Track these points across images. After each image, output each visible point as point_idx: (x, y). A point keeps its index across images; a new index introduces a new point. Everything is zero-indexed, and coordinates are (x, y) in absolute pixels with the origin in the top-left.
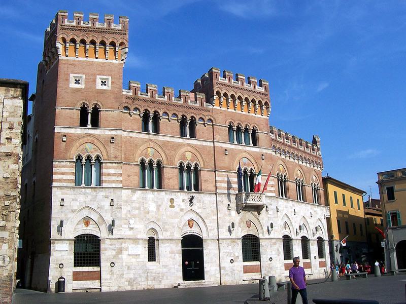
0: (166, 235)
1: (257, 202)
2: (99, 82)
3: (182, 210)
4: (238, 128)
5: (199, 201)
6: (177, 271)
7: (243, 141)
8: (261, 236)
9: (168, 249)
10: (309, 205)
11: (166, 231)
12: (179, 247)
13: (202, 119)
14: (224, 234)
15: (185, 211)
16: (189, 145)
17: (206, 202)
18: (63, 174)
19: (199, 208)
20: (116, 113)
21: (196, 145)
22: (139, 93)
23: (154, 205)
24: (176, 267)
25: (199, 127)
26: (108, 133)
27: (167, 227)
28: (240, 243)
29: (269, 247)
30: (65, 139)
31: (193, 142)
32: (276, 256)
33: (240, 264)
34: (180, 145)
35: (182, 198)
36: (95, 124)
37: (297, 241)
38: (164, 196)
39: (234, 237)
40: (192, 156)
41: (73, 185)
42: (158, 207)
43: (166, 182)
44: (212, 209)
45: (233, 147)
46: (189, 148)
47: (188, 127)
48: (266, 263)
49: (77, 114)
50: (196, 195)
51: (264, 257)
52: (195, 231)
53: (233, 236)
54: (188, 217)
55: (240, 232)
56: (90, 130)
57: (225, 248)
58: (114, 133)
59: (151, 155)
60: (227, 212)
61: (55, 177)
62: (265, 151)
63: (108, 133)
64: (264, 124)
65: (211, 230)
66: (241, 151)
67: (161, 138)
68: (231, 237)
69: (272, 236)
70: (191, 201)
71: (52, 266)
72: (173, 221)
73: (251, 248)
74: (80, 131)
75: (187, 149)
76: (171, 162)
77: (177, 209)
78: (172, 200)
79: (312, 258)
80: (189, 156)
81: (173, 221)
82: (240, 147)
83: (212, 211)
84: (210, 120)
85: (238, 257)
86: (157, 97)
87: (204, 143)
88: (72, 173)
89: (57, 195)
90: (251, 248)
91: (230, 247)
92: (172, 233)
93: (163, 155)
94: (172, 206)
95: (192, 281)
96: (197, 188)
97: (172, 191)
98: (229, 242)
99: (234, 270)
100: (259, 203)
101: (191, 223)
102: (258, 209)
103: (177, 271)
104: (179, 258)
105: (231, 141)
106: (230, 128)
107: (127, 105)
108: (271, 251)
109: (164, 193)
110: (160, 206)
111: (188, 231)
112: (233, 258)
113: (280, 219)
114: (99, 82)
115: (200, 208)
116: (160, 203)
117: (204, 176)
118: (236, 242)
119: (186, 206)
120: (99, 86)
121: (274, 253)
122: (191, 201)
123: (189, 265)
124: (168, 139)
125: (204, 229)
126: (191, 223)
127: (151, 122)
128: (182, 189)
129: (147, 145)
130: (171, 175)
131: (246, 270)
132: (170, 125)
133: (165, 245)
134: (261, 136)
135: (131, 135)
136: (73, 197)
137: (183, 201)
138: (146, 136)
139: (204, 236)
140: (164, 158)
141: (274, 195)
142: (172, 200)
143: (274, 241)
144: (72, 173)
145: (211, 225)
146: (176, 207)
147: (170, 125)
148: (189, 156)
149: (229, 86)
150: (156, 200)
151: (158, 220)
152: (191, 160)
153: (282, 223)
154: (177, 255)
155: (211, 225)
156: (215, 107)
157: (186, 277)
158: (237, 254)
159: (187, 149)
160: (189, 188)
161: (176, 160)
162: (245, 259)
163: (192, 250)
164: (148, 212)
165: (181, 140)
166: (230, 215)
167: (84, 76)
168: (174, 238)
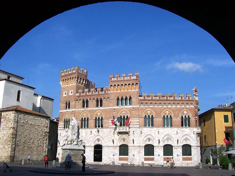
0: (89, 145)
1: (125, 131)
2: (70, 92)
3: (95, 135)
4: (122, 98)
5: (102, 131)
6: (92, 158)
7: (124, 103)
8: (129, 145)
9: (89, 150)
10: (176, 128)
11: (88, 143)
12: (93, 149)
13: (104, 98)
14: (111, 144)
15: (96, 136)
16: (99, 109)
17: (104, 131)
18: (61, 125)
19: (101, 134)
20: (74, 102)
21: (102, 109)
22: (81, 93)
23: (85, 134)
24: (91, 156)
25: (104, 102)
26: (72, 110)
27: (89, 141)
28: (118, 148)
29: (133, 150)
30: (61, 114)
31: (101, 108)
32: (137, 154)
33: (117, 156)
34: (96, 110)
35: (95, 130)
36: (69, 108)
37: (159, 147)
38: (88, 130)
39: (115, 145)
40: (100, 114)
41: (63, 128)
42: (86, 134)
43: (89, 125)
44: (107, 134)
45: (118, 107)
46: (99, 111)
47: (99, 103)
48: (131, 157)
49: (64, 105)
50: (100, 129)
51: (130, 154)
52: (100, 143)
53: (115, 145)
54: (97, 138)
55: (118, 143)
56: (68, 110)
57: (112, 150)
58: (73, 110)
59: (85, 116)
60: (113, 135)
61: (59, 126)
62: (135, 106)
63: (72, 110)
64: (136, 94)
65: (106, 142)
66: (122, 109)
67: (89, 109)
68: (114, 145)
69: (135, 144)
70: (98, 132)
71: (57, 154)
72: (91, 139)
73: (124, 150)
74: (65, 111)
75: (99, 111)
76: (92, 117)
77: (93, 135)
78: (91, 132)
79: (175, 154)
80: (99, 114)
81: (91, 139)
82: (122, 107)
83: (107, 135)
84: (108, 98)
85: (117, 154)
86: (88, 94)
87: (106, 108)
88: (63, 125)
89: (59, 132)
90: (124, 150)
91: (113, 150)
92: (90, 144)
93: (89, 115)
94: (91, 134)
95: (97, 162)
96: (102, 126)
97: (91, 128)
98: (113, 147)
99: (114, 159)
100: (126, 131)
101: (98, 140)
102: (126, 133)
103: (92, 158)
104: (93, 153)
105: (118, 105)
106: (118, 99)
107: (77, 99)
108: (135, 152)
109: (88, 129)
110: (87, 134)
111: (97, 143)
112: (114, 154)
113: (143, 137)
114: (70, 92)
115: (102, 134)
116: (87, 133)
117: (104, 121)
118: (116, 147)
119: (96, 133)
120: (70, 94)
121: (136, 152)
122: (98, 132)
123: (97, 155)
124: (91, 109)
125: (103, 142)
126: (98, 140)
127: (85, 104)
128: (96, 127)
129: (85, 112)
130: (92, 122)
131: (120, 159)
132: (92, 102)
133: (88, 148)
134: (133, 99)
135: (78, 109)
136: (62, 133)
137: (95, 132)
138: (83, 109)
139: (103, 145)
140: (89, 117)
141: (138, 126)
142: (91, 132)
143: (136, 147)
144: (63, 125)
145: (106, 140)
146: (93, 134)
147: (92, 102)
148: (99, 114)
149: (118, 81)
150: (85, 132)
151: (86, 139)
152: (100, 116)
153: (146, 139)
154: (92, 152)
155: (106, 140)
156: (111, 92)
157: (95, 160)
158: (116, 153)
159: (99, 111)
160: (99, 127)
161: (94, 116)
162: (120, 155)
163: (98, 150)
164: (83, 136)
165: (96, 108)
166: (114, 136)
167: (66, 91)
168: (92, 145)
